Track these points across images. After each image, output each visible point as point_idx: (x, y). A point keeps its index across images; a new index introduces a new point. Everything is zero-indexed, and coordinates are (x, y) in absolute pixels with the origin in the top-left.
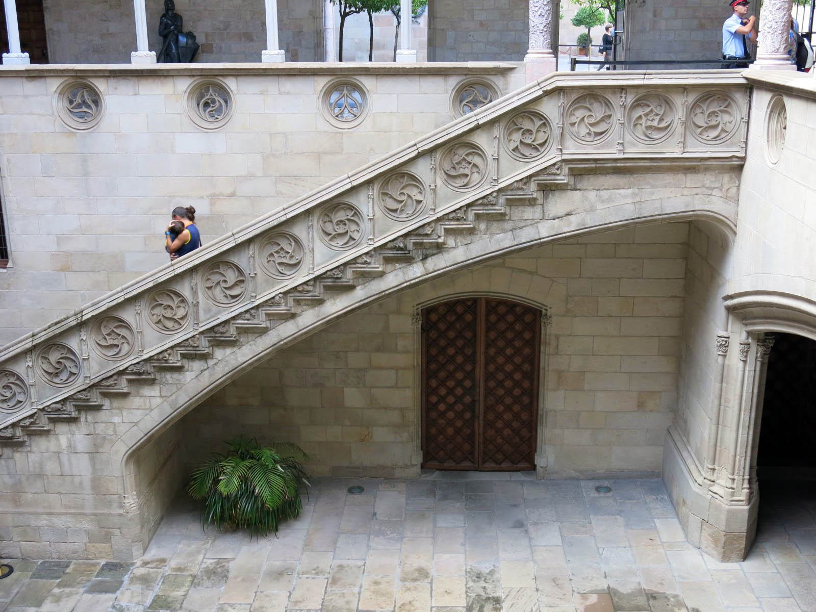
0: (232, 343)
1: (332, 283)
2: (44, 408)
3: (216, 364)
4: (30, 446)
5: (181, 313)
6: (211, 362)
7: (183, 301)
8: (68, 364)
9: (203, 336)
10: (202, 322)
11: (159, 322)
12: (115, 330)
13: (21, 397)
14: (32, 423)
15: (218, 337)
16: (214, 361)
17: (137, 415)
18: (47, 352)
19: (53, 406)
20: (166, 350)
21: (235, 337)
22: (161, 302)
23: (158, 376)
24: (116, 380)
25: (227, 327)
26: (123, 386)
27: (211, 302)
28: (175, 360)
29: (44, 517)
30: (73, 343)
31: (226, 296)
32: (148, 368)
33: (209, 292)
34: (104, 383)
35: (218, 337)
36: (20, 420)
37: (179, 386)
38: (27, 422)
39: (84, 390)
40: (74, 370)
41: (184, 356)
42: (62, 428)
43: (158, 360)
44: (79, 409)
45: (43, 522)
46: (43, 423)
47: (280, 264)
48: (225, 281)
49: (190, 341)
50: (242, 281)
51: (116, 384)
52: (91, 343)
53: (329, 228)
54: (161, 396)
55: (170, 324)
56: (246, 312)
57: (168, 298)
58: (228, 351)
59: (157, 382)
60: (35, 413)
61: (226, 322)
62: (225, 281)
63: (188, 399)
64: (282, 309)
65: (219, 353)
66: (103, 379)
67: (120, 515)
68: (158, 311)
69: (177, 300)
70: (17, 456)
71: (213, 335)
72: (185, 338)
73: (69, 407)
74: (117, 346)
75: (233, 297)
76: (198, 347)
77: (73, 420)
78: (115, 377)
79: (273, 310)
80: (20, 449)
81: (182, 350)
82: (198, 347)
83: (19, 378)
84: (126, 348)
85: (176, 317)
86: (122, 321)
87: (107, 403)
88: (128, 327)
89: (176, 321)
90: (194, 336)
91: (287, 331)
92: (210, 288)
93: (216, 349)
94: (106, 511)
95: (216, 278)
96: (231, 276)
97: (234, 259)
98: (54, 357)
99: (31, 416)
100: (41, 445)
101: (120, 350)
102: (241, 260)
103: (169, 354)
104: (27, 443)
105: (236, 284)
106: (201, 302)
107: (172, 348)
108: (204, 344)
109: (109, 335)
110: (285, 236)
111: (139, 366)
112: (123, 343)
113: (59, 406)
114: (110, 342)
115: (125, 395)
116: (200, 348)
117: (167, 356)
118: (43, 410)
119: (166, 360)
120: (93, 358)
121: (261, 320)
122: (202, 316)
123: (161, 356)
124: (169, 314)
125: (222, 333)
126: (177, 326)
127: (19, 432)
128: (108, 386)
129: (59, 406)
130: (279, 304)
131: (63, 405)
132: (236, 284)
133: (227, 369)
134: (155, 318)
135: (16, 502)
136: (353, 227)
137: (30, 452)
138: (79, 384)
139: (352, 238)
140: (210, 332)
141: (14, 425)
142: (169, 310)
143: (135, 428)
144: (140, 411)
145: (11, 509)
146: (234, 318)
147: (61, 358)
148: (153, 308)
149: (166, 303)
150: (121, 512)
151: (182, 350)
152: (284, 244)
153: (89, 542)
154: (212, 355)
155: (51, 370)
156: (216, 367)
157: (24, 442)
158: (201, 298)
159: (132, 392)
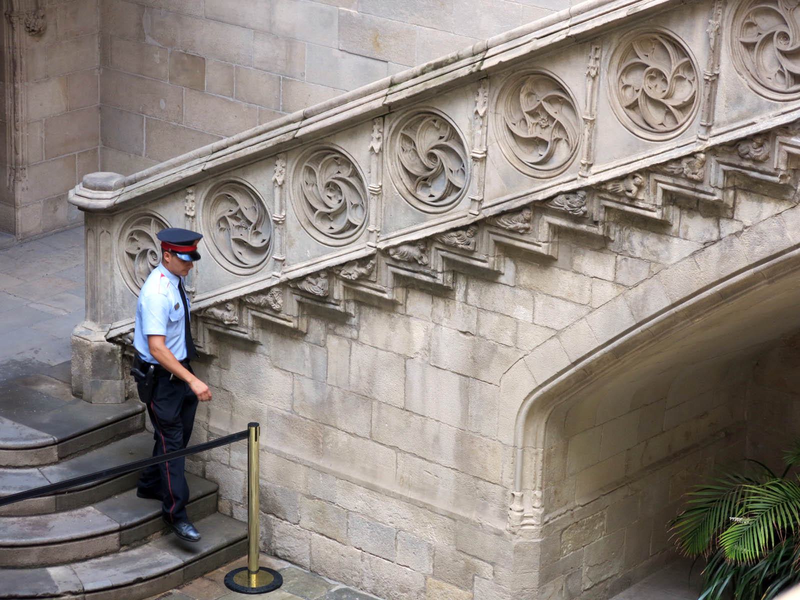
2: (387, 250)
3: (737, 234)
4: (358, 327)
5: (682, 94)
6: (728, 228)
7: (689, 66)
8: (449, 163)
9: (713, 160)
10: (718, 126)
11: (634, 106)
12: (546, 106)
13: (355, 217)
14: (362, 277)
16: (735, 227)
17: (563, 314)
18: (412, 127)
19: (405, 249)
20: (633, 175)
21: (782, 177)
22: (644, 60)
23: (615, 234)
24: (528, 221)
25: (767, 147)
26: (540, 239)
27: (745, 81)
29: (360, 491)
31: (781, 73)
32: (594, 208)
33: (749, 58)
34: (504, 222)
36: (342, 265)
37: (655, 267)
38: (354, 273)
39: (465, 228)
40: (458, 181)
41: (671, 198)
42: (418, 304)
43: (614, 193)
44: (457, 269)
45: (355, 501)
46: (383, 284)
48: (785, 36)
49: (684, 164)
51: (527, 229)
52: (496, 126)
54: (615, 283)
55: (656, 116)
57: (658, 51)
58: (769, 208)
59: (611, 246)
60: (371, 257)
61: (766, 136)
62: (785, 36)
63: (667, 303)
65: (749, 210)
66: (503, 213)
67: (499, 534)
68: (637, 79)
69: (677, 62)
70: (333, 341)
71: (736, 160)
72: (675, 154)
73: (435, 260)
74: (544, 143)
76: (700, 182)
77: (441, 292)
78: (527, 214)
80: (339, 330)
81: (666, 183)
82: (700, 182)
83: (355, 174)
84: (562, 153)
85: (669, 103)
86: (562, 89)
87: (508, 269)
89: (669, 113)
90: (693, 155)
92: (749, 46)
93: (742, 198)
94: (473, 516)
95: (767, 24)
98: (427, 139)
100: (375, 329)
101: (549, 156)
103: (640, 187)
104: (354, 321)
106: (722, 76)
107: (646, 172)
109: (533, 114)
111: (576, 200)
112: (558, 140)
113: (414, 252)
114: (536, 133)
115: (545, 262)
116: (705, 187)
117: (634, 189)
118: (385, 252)
119: (633, 199)
120: (494, 158)
122: (721, 111)
123: (621, 187)
125: (755, 160)
126: (670, 125)
127: (338, 292)
128: (512, 231)
129: (414, 252)
131: (423, 251)
133: (761, 252)
134: (629, 96)
135: (319, 445)
137: (356, 340)
138: (463, 212)
140: (730, 153)
141: (331, 272)
142: (658, 82)
143: (554, 342)
144: (570, 307)
145: (306, 456)
147: (436, 147)
148: (627, 71)
149: (653, 65)
150: (502, 526)
151: (666, 183)
153: (433, 576)
154: (733, 209)
155: (416, 170)
156: (736, 241)
159: (562, 258)
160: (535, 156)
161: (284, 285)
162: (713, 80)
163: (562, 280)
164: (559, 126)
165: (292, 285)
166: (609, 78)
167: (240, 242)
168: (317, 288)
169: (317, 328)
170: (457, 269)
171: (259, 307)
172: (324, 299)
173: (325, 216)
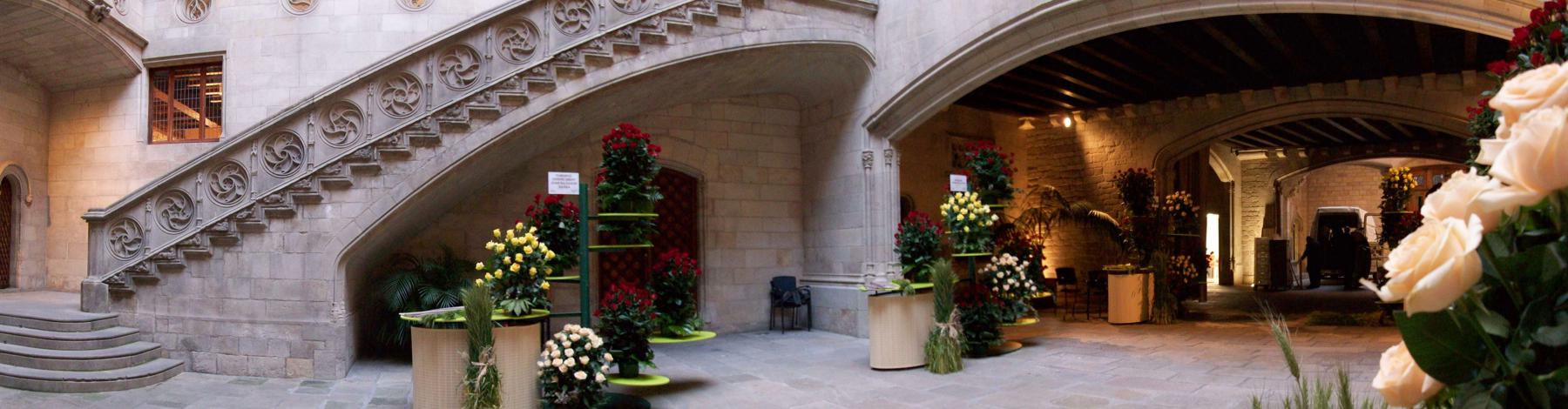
0: (464, 128)
1: (563, 65)
5: (412, 98)
6: (440, 150)
11: (390, 108)
14: (249, 216)
15: (450, 120)
28: (404, 144)
29: (247, 326)
30: (301, 130)
34: (328, 170)
35: (450, 120)
38: (244, 214)
42: (277, 226)
45: (244, 331)
47: (515, 51)
50: (476, 67)
52: (317, 131)
53: (561, 17)
56: (481, 92)
61: (459, 104)
64: (517, 92)
65: (447, 140)
67: (327, 325)
70: (227, 256)
73: (289, 199)
75: (467, 82)
77: (289, 215)
79: (507, 93)
83: (242, 171)
84: (352, 136)
87: (325, 195)
88: (358, 115)
91: (514, 118)
92: (443, 73)
94: (312, 321)
95: (451, 64)
96: (466, 62)
97: (471, 43)
98: (278, 147)
99: (248, 208)
100: (250, 244)
102: (478, 44)
105: (469, 71)
107: (402, 131)
108: (434, 128)
110: (519, 23)
118: (261, 201)
121: (494, 103)
124: (400, 99)
127: (234, 227)
130: (513, 87)
132: (469, 71)
133: (455, 158)
134: (386, 105)
136: (583, 18)
138: (304, 172)
139: (583, 28)
141: (230, 218)
145: (216, 317)
146: (468, 99)
150: (329, 321)
151: (411, 133)
152: (519, 31)
157: (236, 240)
158: (435, 80)
160: (337, 141)
161: (202, 231)
162: (429, 86)
163: (355, 194)
164: (352, 125)
165: (207, 231)
166: (377, 97)
167: (174, 221)
168: (221, 228)
169: (218, 252)
170: (299, 201)
171: (188, 246)
172: (224, 233)
173: (223, 196)
